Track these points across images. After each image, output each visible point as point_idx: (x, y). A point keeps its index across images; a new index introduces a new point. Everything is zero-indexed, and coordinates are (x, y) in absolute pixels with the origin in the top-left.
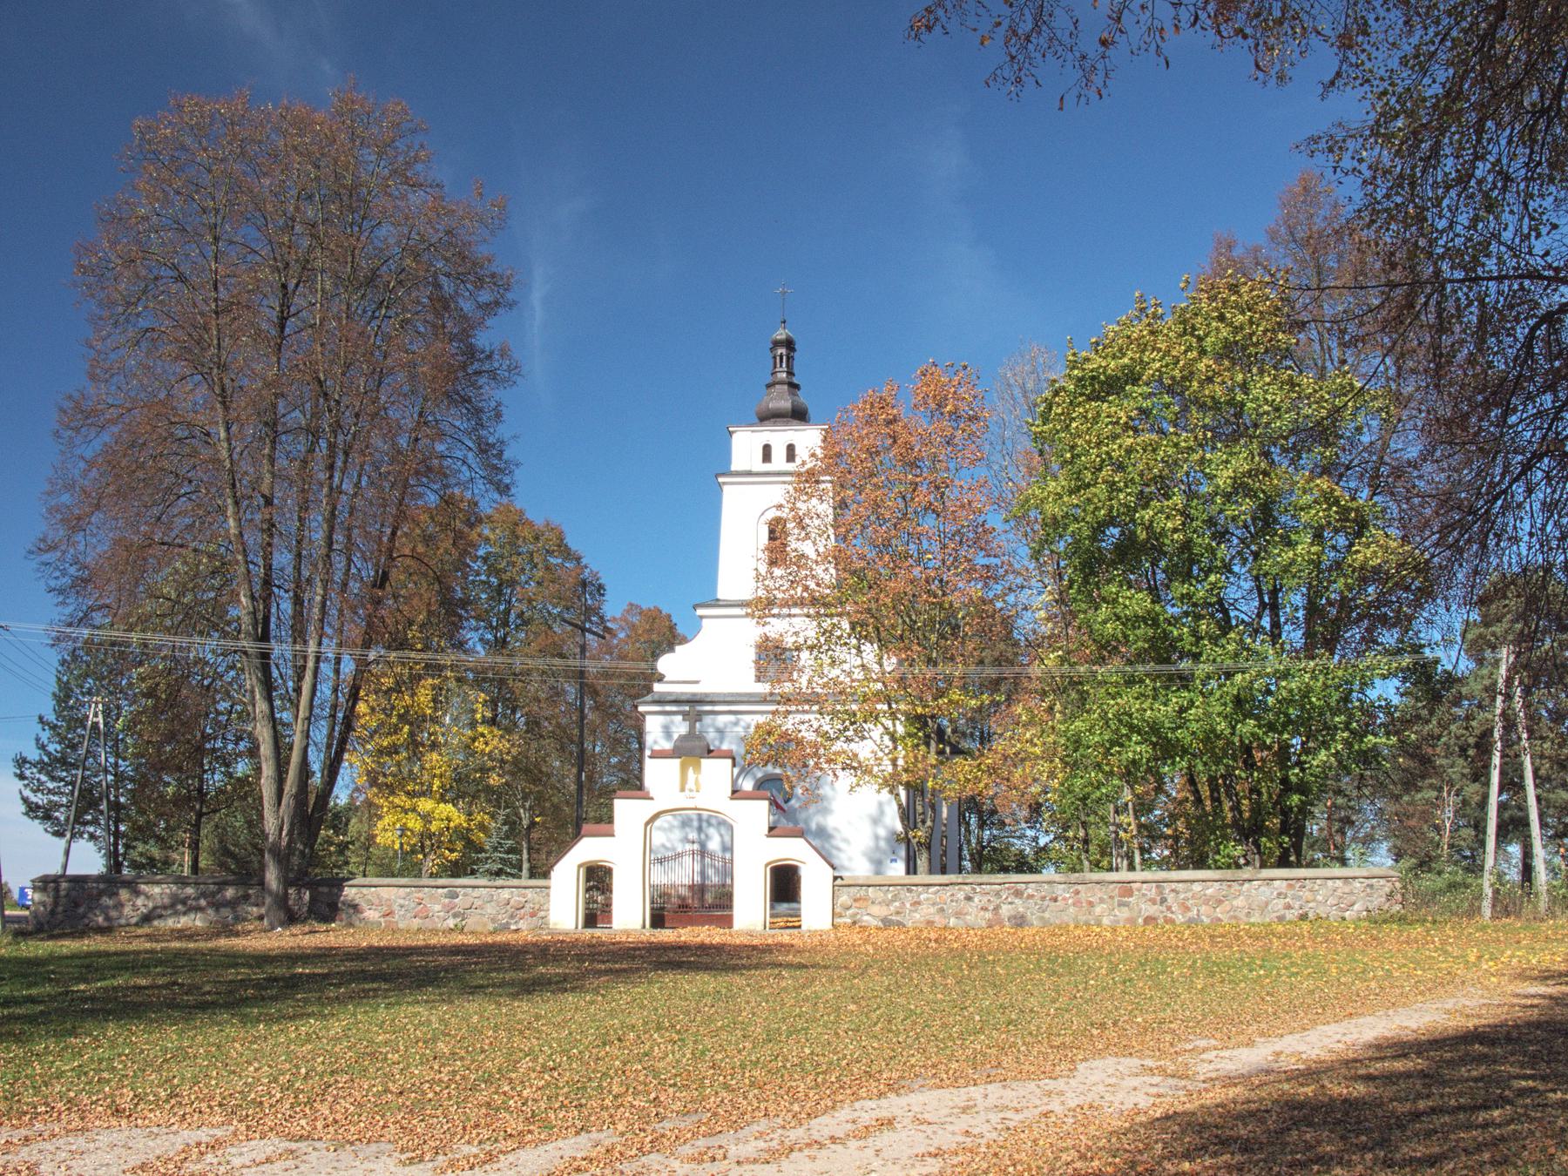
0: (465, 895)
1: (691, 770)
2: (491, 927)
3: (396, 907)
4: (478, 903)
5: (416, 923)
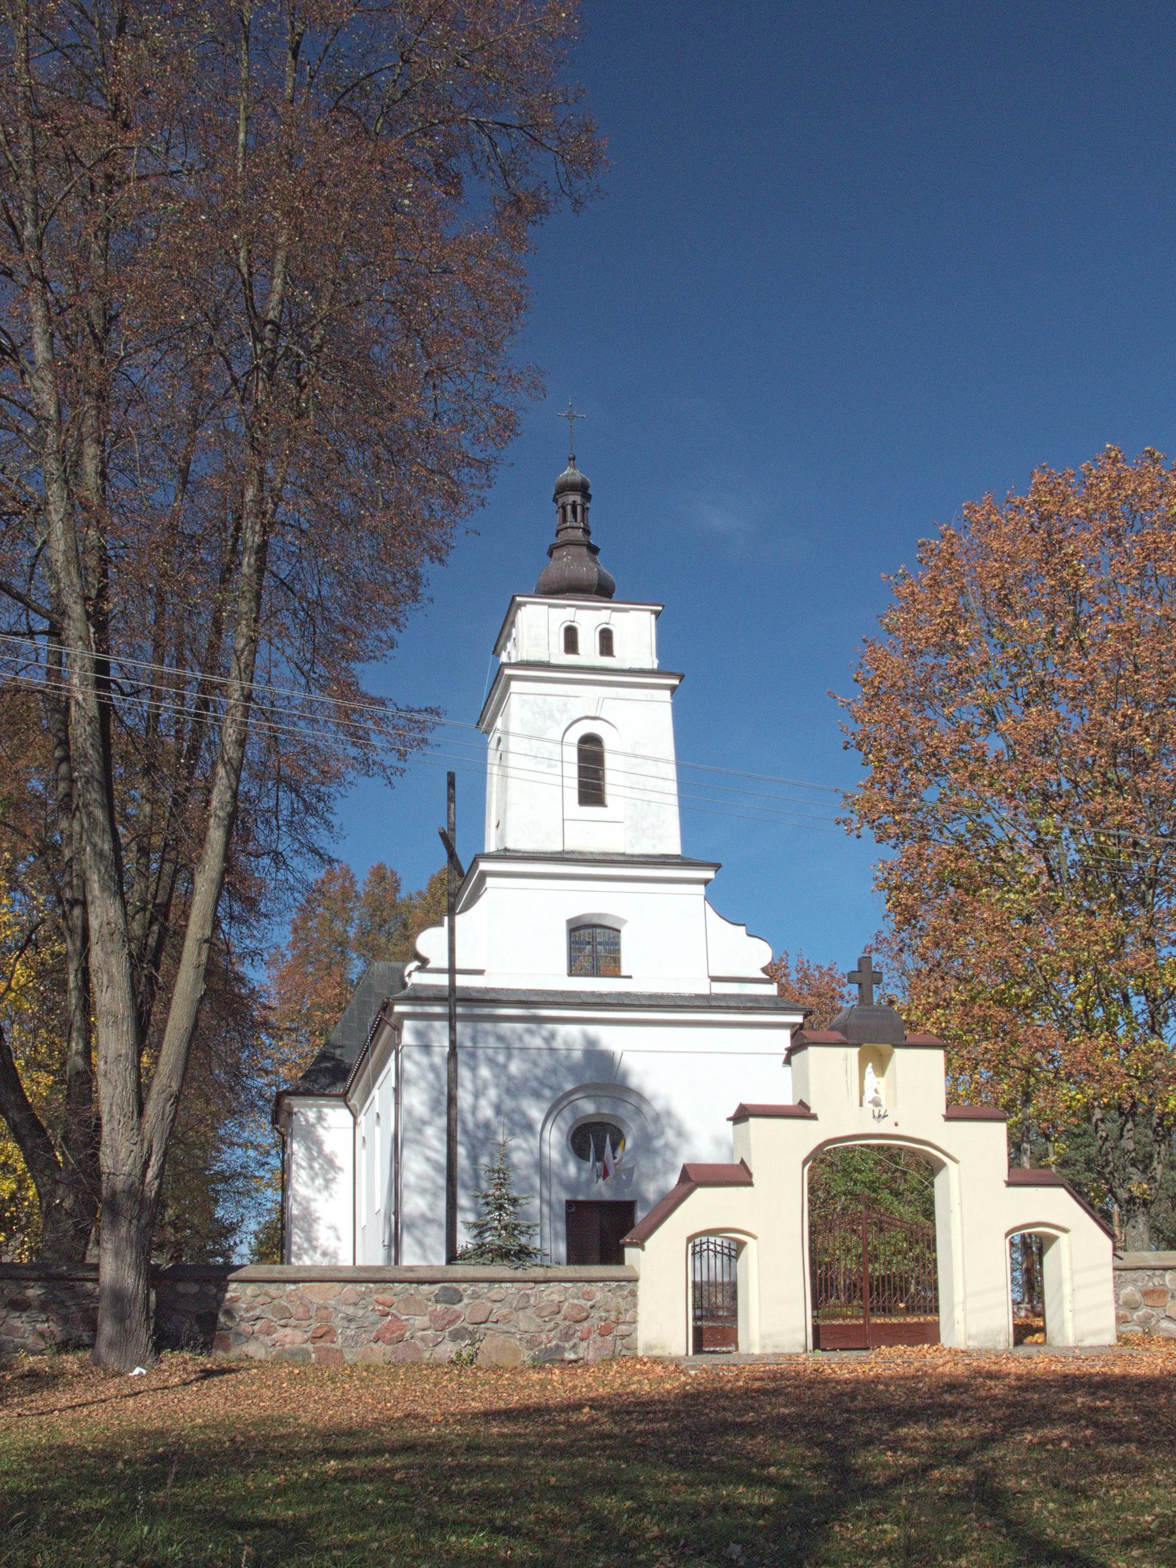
0: (475, 1296)
1: (869, 1069)
2: (526, 1356)
3: (337, 1322)
4: (500, 1311)
5: (380, 1352)
